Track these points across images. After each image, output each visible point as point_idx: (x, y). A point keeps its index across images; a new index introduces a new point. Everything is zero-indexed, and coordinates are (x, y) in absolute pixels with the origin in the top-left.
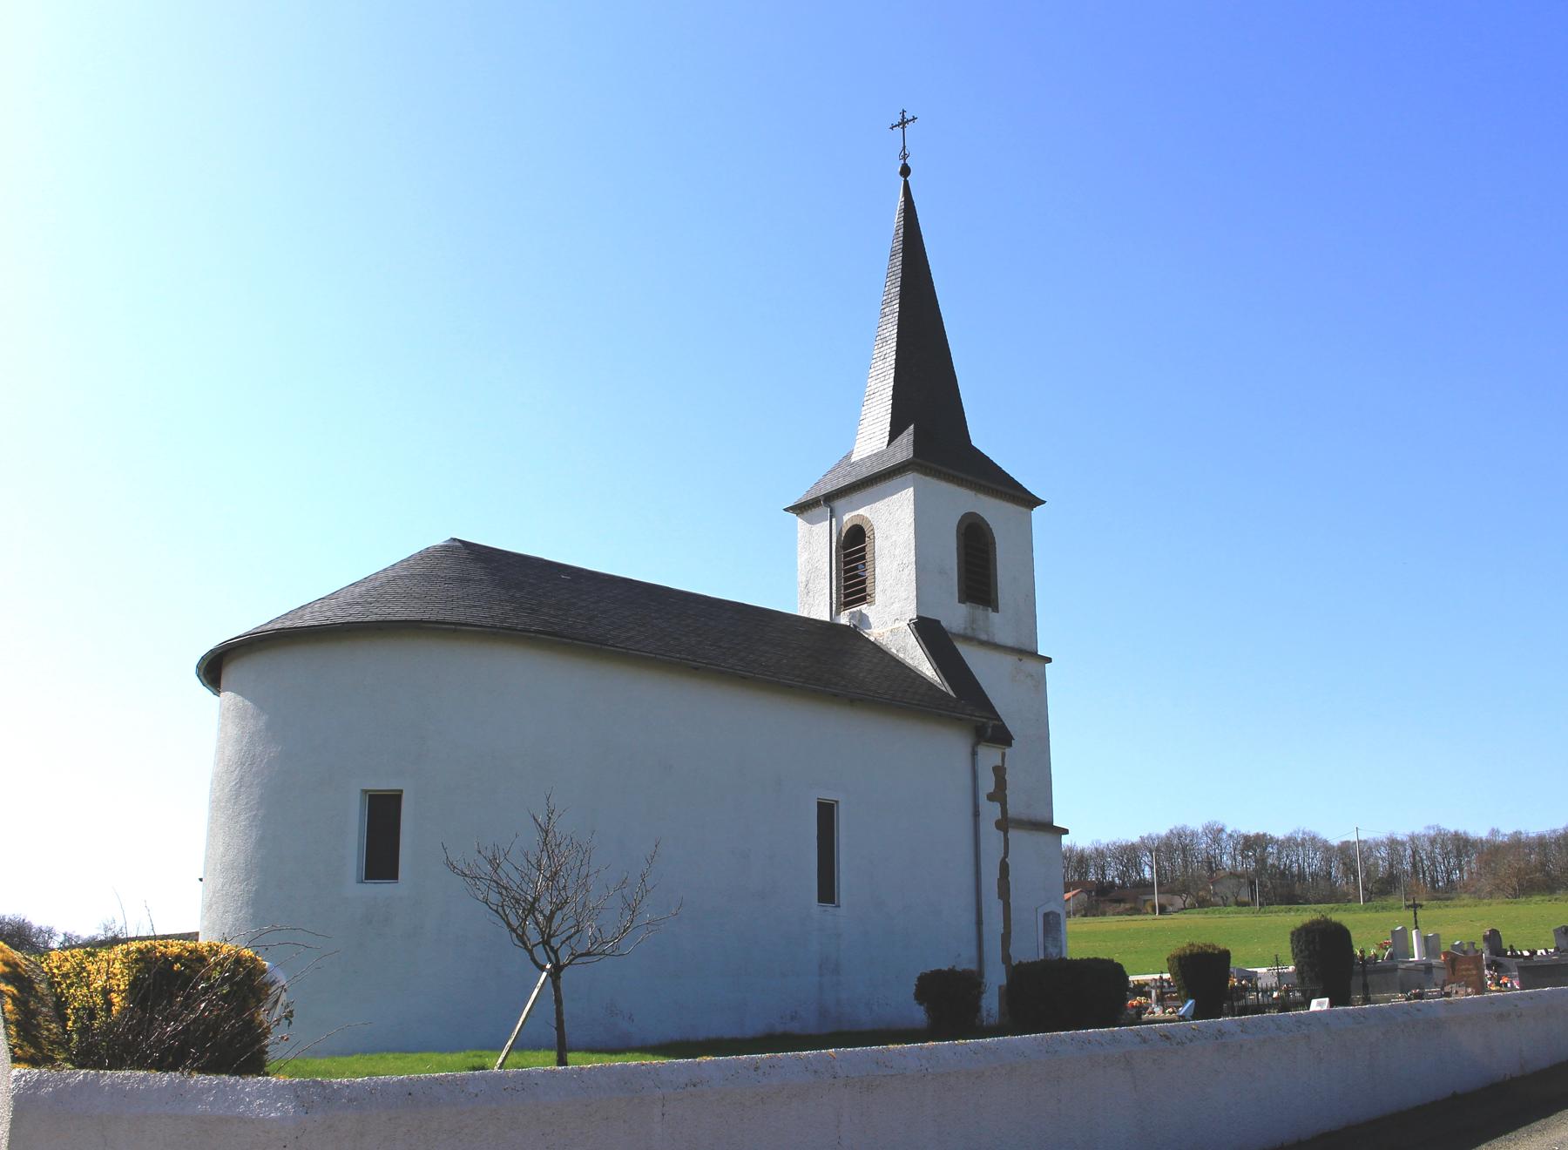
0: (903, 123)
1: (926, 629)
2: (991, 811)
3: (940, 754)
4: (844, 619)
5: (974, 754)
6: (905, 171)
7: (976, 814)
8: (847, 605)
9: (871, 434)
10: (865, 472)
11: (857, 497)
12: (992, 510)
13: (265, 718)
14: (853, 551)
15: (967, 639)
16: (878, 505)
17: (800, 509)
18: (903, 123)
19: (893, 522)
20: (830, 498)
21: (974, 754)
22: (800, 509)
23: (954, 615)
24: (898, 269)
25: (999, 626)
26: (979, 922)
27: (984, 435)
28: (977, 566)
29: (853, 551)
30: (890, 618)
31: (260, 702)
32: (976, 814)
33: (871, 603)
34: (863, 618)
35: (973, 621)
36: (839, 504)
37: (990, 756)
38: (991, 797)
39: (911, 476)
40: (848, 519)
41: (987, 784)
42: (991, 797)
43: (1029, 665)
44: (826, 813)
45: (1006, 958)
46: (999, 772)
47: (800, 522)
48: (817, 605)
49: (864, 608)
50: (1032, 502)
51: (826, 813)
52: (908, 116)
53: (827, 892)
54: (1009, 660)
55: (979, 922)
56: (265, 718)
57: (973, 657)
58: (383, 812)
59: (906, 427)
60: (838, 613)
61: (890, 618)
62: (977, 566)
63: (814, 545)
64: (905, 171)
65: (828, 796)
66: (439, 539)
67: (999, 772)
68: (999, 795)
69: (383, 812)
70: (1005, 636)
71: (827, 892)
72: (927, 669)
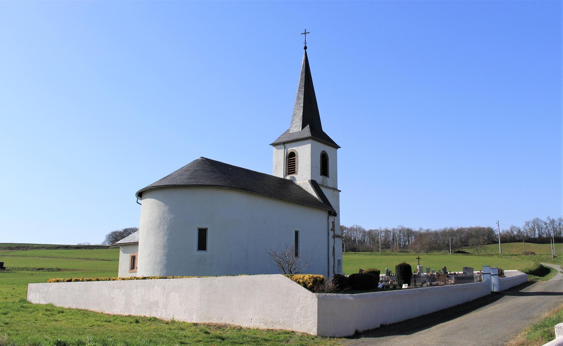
0: (305, 33)
1: (313, 183)
2: (331, 233)
3: (319, 218)
4: (288, 178)
5: (328, 218)
6: (306, 48)
7: (328, 234)
8: (289, 174)
9: (296, 127)
10: (295, 137)
11: (293, 144)
12: (328, 149)
13: (168, 207)
14: (291, 159)
15: (323, 186)
16: (300, 147)
17: (274, 145)
18: (305, 33)
19: (305, 154)
20: (284, 143)
21: (328, 218)
22: (274, 145)
23: (319, 179)
24: (304, 77)
25: (329, 182)
26: (328, 262)
27: (326, 128)
28: (324, 165)
29: (291, 159)
30: (303, 178)
31: (166, 203)
32: (328, 234)
33: (297, 174)
34: (294, 178)
35: (323, 181)
36: (287, 145)
37: (332, 219)
38: (331, 230)
39: (310, 141)
40: (290, 150)
41: (331, 227)
42: (331, 230)
43: (336, 192)
44: (297, 233)
45: (334, 272)
46: (333, 223)
47: (274, 148)
48: (279, 172)
49: (294, 175)
50: (337, 147)
51: (297, 233)
52: (307, 32)
53: (297, 255)
54: (331, 191)
55: (328, 262)
56: (168, 207)
57: (324, 190)
58: (202, 234)
59: (306, 125)
60: (286, 176)
61: (303, 178)
62: (324, 165)
63: (279, 155)
64: (306, 48)
65: (297, 230)
66: (198, 157)
67: (333, 223)
68: (333, 229)
69: (202, 234)
70: (330, 185)
71: (297, 255)
72: (314, 194)
